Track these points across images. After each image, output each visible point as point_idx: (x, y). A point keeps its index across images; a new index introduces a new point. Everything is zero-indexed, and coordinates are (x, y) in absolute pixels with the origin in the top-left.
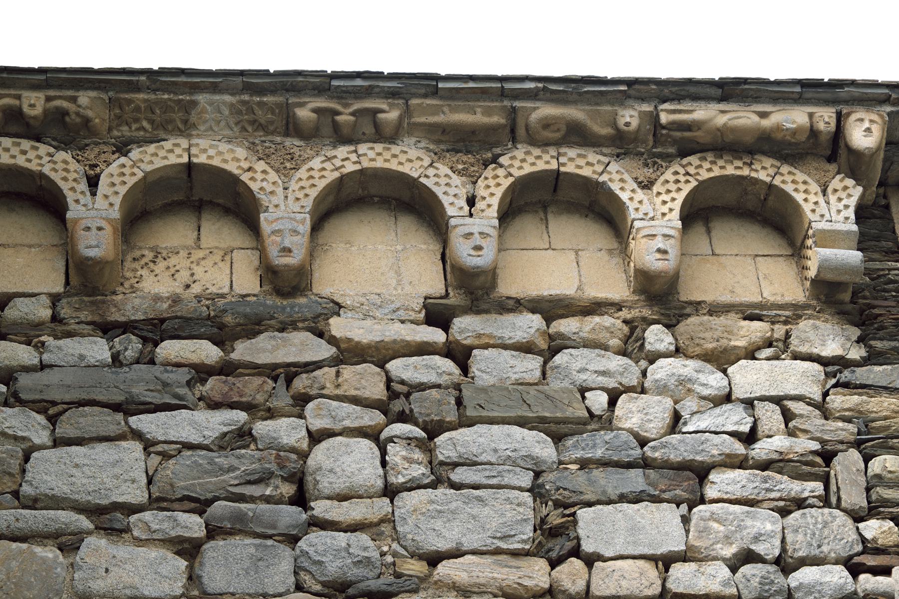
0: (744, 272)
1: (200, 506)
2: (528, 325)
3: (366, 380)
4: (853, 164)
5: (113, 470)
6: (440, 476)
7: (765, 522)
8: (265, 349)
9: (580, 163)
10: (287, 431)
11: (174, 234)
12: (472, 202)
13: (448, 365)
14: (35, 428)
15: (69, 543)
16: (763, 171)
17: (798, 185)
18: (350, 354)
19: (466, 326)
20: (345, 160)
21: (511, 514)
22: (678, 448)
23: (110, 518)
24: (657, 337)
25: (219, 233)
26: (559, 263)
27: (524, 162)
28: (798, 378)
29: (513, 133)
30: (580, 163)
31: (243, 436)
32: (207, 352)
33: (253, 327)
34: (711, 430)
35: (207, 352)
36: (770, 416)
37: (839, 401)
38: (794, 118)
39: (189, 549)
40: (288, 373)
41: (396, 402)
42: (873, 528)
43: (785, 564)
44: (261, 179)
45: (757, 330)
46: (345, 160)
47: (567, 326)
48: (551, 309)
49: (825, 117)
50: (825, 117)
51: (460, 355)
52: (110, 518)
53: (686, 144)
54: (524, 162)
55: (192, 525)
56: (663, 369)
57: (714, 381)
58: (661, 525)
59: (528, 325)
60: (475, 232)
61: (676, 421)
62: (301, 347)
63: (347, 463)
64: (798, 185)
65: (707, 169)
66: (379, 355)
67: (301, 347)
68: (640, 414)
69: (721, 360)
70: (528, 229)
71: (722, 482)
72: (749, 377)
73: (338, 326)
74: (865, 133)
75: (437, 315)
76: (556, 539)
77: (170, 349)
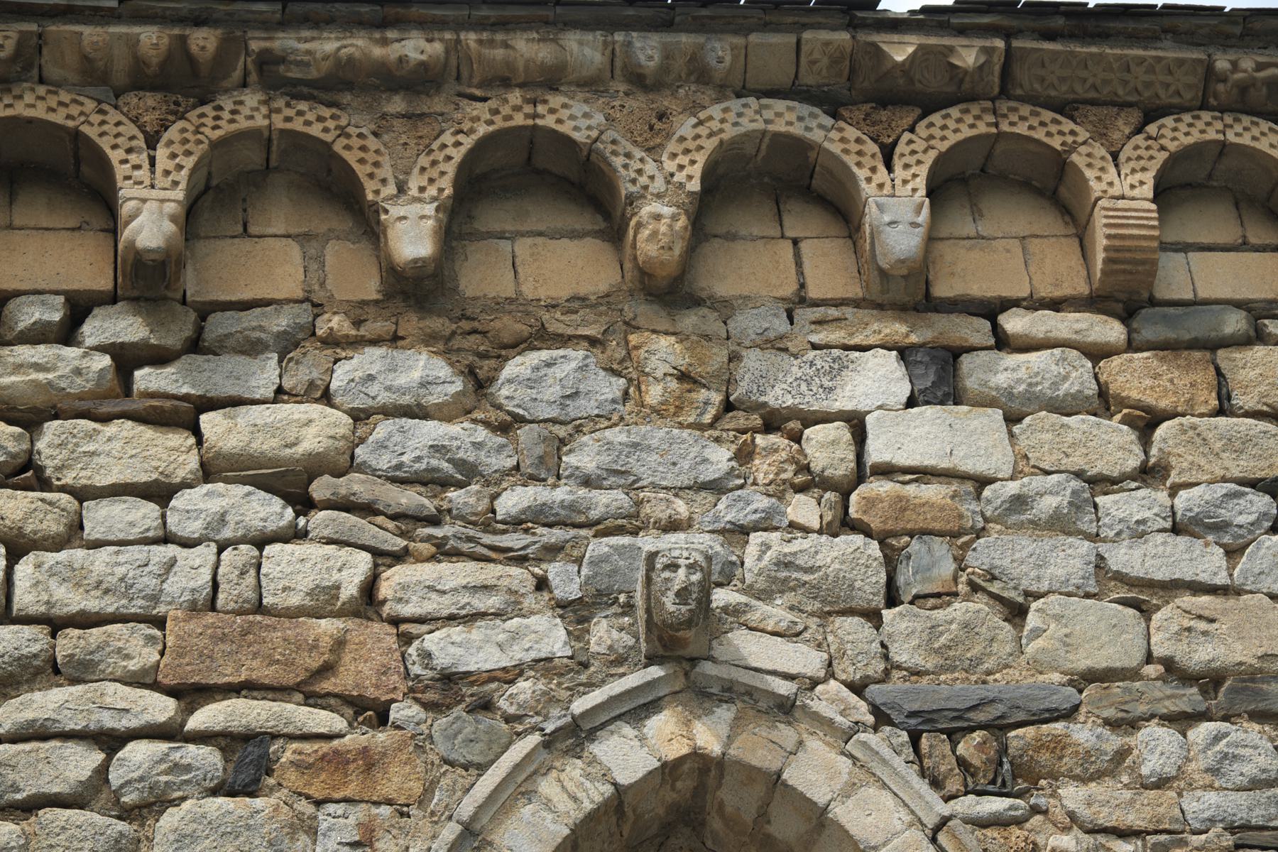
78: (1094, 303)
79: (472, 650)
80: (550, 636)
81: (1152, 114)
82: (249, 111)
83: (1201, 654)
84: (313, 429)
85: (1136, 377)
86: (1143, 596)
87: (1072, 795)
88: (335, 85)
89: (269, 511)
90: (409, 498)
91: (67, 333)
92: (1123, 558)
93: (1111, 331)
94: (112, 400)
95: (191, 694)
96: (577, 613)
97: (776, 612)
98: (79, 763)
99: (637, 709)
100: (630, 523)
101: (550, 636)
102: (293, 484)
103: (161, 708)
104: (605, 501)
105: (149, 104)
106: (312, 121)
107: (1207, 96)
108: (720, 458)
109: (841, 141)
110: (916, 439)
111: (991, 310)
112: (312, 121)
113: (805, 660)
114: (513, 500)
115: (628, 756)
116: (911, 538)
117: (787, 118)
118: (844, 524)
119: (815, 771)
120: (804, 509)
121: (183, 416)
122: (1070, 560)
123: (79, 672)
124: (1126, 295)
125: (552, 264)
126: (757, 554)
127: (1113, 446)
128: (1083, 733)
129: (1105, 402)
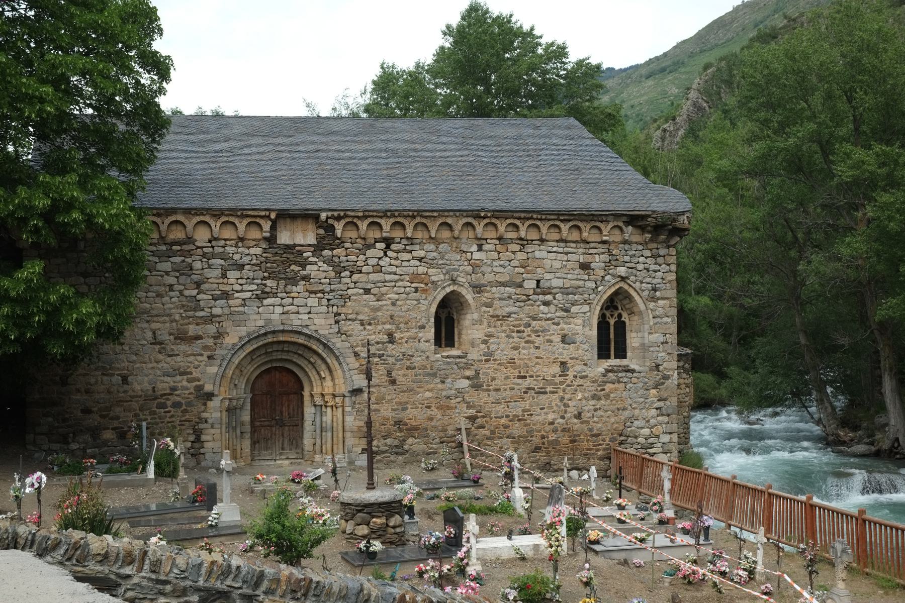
0: (255, 234)
1: (178, 271)
2: (222, 243)
3: (199, 251)
4: (271, 220)
5: (166, 266)
6: (209, 267)
7: (251, 274)
8: (185, 247)
9: (231, 219)
10: (189, 260)
11: (174, 227)
12: (216, 225)
13: (211, 249)
14: (156, 260)
15: (162, 276)
16: (257, 220)
17: (262, 222)
18: (198, 247)
19: (214, 243)
20: (198, 219)
21: (218, 272)
22: (240, 262)
23: (167, 273)
24: (240, 244)
25: (180, 228)
26: (228, 233)
27: (224, 219)
28: (258, 251)
29: (222, 214)
30: (231, 219)
31: (184, 261)
32: (179, 248)
33: (185, 244)
34: (246, 259)
35: (179, 248)
36: (254, 257)
37: (264, 255)
38: (263, 213)
39: (177, 277)
40: (189, 251)
41: (204, 255)
42: (266, 274)
43: (253, 279)
44: (186, 222)
45: (254, 243)
46: (198, 219)
47: (228, 242)
48: (226, 240)
49: (267, 213)
50: (267, 213)
51: (213, 247)
52: (167, 273)
53: (247, 216)
54: (224, 219)
55: (178, 274)
56: (241, 250)
57: (247, 252)
58: (237, 274)
59: (222, 243)
60: (216, 230)
61: (241, 258)
62: (191, 247)
63: (198, 265)
64: (262, 222)
65: (250, 220)
66: (202, 248)
67: (191, 247)
68: (237, 257)
69: (248, 248)
70: (224, 227)
71: (247, 267)
72: (253, 251)
73: (196, 244)
74: (273, 216)
75: (210, 241)
76: (224, 276)
77: (174, 247)
78: (497, 239)
79: (434, 278)
80: (442, 277)
81: (506, 219)
82: (418, 220)
83: (500, 280)
84: (422, 254)
85: (499, 248)
86: (496, 273)
87: (486, 294)
88: (426, 217)
89: (418, 263)
90: (431, 262)
91: (399, 243)
92: (495, 269)
93: (497, 242)
94: (404, 251)
95: (412, 283)
96: (445, 275)
97: (462, 275)
98: (403, 290)
99: (449, 285)
100: (451, 265)
101: (442, 277)
102: (420, 260)
103: (409, 284)
104: (448, 262)
105: (409, 219)
106: (424, 221)
107: (512, 217)
108: (459, 257)
109: (475, 223)
110: (478, 256)
111: (486, 239)
112: (424, 221)
113: (464, 280)
114: (440, 262)
115: (448, 290)
116: (476, 267)
117: (470, 220)
118: (469, 265)
119: (464, 292)
120: (466, 263)
121: (410, 252)
122: (489, 269)
123: (402, 281)
124: (500, 239)
125: (446, 234)
126: (462, 268)
127: (495, 255)
128: (488, 288)
129: (496, 250)
